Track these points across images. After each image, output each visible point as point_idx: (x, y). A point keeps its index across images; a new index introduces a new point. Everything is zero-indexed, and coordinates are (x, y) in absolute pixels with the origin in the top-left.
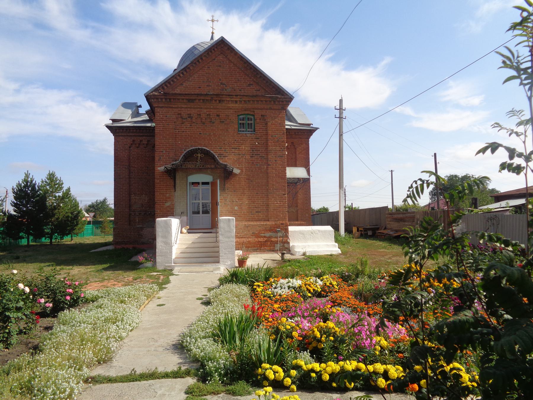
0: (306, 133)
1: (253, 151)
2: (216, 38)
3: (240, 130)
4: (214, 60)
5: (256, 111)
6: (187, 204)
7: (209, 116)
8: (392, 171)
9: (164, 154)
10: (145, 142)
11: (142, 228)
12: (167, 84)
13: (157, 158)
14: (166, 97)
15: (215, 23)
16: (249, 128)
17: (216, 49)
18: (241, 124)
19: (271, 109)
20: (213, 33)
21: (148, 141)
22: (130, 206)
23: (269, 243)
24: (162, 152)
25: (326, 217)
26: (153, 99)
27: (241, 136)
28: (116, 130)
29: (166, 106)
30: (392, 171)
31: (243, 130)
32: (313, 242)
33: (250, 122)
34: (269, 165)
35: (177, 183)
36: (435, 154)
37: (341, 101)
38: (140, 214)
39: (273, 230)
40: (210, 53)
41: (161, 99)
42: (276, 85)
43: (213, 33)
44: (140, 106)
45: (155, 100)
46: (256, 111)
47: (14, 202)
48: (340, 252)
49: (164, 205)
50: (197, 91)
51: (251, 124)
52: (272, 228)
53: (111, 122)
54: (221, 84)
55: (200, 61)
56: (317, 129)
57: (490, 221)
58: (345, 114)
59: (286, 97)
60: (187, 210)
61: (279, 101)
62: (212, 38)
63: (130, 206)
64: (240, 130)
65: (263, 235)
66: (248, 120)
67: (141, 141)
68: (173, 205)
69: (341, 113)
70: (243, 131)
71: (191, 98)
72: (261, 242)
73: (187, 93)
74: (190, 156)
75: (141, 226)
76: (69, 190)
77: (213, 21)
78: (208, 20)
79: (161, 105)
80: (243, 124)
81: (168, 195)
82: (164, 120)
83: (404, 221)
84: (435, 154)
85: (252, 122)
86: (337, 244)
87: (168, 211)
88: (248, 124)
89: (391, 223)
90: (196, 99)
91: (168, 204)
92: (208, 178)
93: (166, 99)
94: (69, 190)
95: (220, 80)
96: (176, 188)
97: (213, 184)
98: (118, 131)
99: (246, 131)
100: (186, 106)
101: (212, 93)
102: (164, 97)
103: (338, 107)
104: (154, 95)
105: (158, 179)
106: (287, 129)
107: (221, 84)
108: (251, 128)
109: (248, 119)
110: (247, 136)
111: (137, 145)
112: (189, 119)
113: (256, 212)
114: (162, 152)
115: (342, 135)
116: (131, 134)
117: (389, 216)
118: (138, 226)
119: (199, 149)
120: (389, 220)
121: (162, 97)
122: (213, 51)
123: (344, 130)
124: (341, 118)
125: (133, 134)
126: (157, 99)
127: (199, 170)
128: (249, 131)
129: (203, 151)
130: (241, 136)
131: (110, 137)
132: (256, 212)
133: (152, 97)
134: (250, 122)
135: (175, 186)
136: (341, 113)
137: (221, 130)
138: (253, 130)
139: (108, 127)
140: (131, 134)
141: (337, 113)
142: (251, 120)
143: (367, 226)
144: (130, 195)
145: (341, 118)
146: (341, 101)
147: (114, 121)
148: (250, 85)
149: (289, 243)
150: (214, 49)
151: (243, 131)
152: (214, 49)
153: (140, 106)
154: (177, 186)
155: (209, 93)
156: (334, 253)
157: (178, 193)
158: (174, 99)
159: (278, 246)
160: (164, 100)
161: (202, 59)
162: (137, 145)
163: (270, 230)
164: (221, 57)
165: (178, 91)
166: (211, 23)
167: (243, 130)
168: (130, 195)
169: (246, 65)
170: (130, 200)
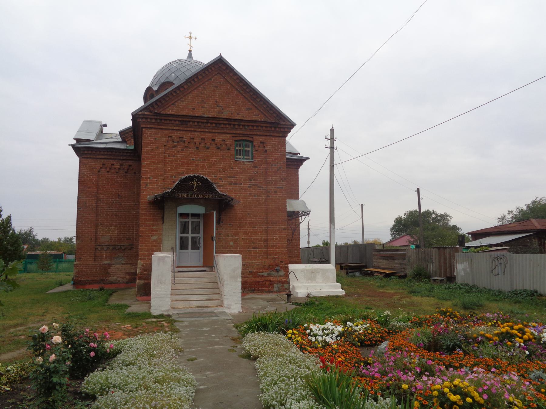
0: (296, 162)
1: (250, 180)
2: (205, 57)
3: (237, 157)
4: (210, 79)
6: (176, 238)
7: (203, 141)
8: (362, 205)
9: (152, 180)
10: (117, 166)
11: (110, 265)
12: (158, 103)
13: (143, 185)
14: (156, 117)
15: (193, 40)
16: (246, 156)
17: (213, 68)
18: (237, 150)
19: (271, 136)
20: (190, 51)
21: (121, 165)
22: (96, 239)
23: (267, 283)
24: (150, 178)
25: (319, 255)
26: (142, 118)
27: (238, 164)
28: (84, 151)
29: (156, 127)
30: (362, 205)
31: (240, 157)
32: (313, 281)
33: (247, 149)
34: (267, 196)
35: (165, 215)
36: (418, 189)
37: (332, 130)
38: (107, 248)
39: (272, 268)
40: (207, 73)
41: (151, 119)
42: (277, 111)
43: (190, 51)
44: (105, 126)
45: (144, 120)
47: (61, 240)
48: (344, 293)
50: (191, 113)
51: (249, 151)
52: (271, 267)
53: (75, 142)
54: (217, 106)
55: (196, 80)
56: (308, 158)
57: (496, 260)
58: (336, 144)
59: (288, 123)
60: (176, 245)
61: (280, 128)
62: (190, 56)
63: (96, 239)
64: (237, 157)
65: (261, 274)
66: (246, 147)
67: (113, 165)
68: (161, 239)
69: (332, 143)
70: (240, 158)
71: (185, 119)
72: (259, 282)
73: (179, 114)
74: (185, 184)
75: (108, 262)
76: (9, 218)
77: (190, 38)
78: (185, 37)
79: (149, 126)
80: (240, 150)
82: (154, 143)
83: (394, 259)
84: (418, 189)
85: (250, 149)
86: (340, 284)
87: (155, 246)
88: (246, 151)
89: (378, 261)
90: (189, 121)
91: (154, 238)
92: (200, 210)
93: (156, 119)
94: (9, 218)
95: (216, 102)
96: (165, 219)
97: (207, 217)
98: (86, 152)
99: (243, 159)
100: (178, 128)
101: (207, 116)
103: (329, 137)
105: (144, 209)
106: (287, 159)
107: (217, 106)
108: (248, 156)
109: (246, 146)
110: (244, 164)
111: (108, 170)
112: (181, 143)
113: (254, 248)
114: (150, 178)
115: (333, 166)
116: (101, 157)
117: (377, 253)
118: (105, 262)
119: (195, 176)
120: (376, 257)
121: (152, 117)
122: (210, 71)
123: (336, 161)
124: (332, 148)
125: (103, 157)
126: (147, 118)
127: (191, 201)
128: (246, 159)
129: (200, 179)
130: (238, 164)
131: (75, 160)
132: (254, 248)
133: (141, 116)
134: (247, 149)
135: (163, 218)
136: (332, 143)
137: (216, 156)
138: (250, 157)
139: (74, 146)
140: (101, 157)
141: (328, 143)
142: (249, 147)
143: (356, 262)
144: (97, 225)
145: (332, 148)
146: (332, 130)
147: (78, 140)
148: (248, 109)
149: (289, 283)
150: (211, 68)
151: (240, 158)
152: (211, 68)
153: (105, 126)
154: (165, 217)
155: (204, 116)
156: (339, 294)
157: (166, 226)
158: (165, 120)
159: (276, 287)
160: (153, 121)
161: (197, 77)
162: (108, 170)
163: (269, 269)
164: (218, 78)
165: (169, 111)
166: (188, 39)
167: (240, 157)
168: (97, 225)
169: (245, 87)
170: (96, 232)
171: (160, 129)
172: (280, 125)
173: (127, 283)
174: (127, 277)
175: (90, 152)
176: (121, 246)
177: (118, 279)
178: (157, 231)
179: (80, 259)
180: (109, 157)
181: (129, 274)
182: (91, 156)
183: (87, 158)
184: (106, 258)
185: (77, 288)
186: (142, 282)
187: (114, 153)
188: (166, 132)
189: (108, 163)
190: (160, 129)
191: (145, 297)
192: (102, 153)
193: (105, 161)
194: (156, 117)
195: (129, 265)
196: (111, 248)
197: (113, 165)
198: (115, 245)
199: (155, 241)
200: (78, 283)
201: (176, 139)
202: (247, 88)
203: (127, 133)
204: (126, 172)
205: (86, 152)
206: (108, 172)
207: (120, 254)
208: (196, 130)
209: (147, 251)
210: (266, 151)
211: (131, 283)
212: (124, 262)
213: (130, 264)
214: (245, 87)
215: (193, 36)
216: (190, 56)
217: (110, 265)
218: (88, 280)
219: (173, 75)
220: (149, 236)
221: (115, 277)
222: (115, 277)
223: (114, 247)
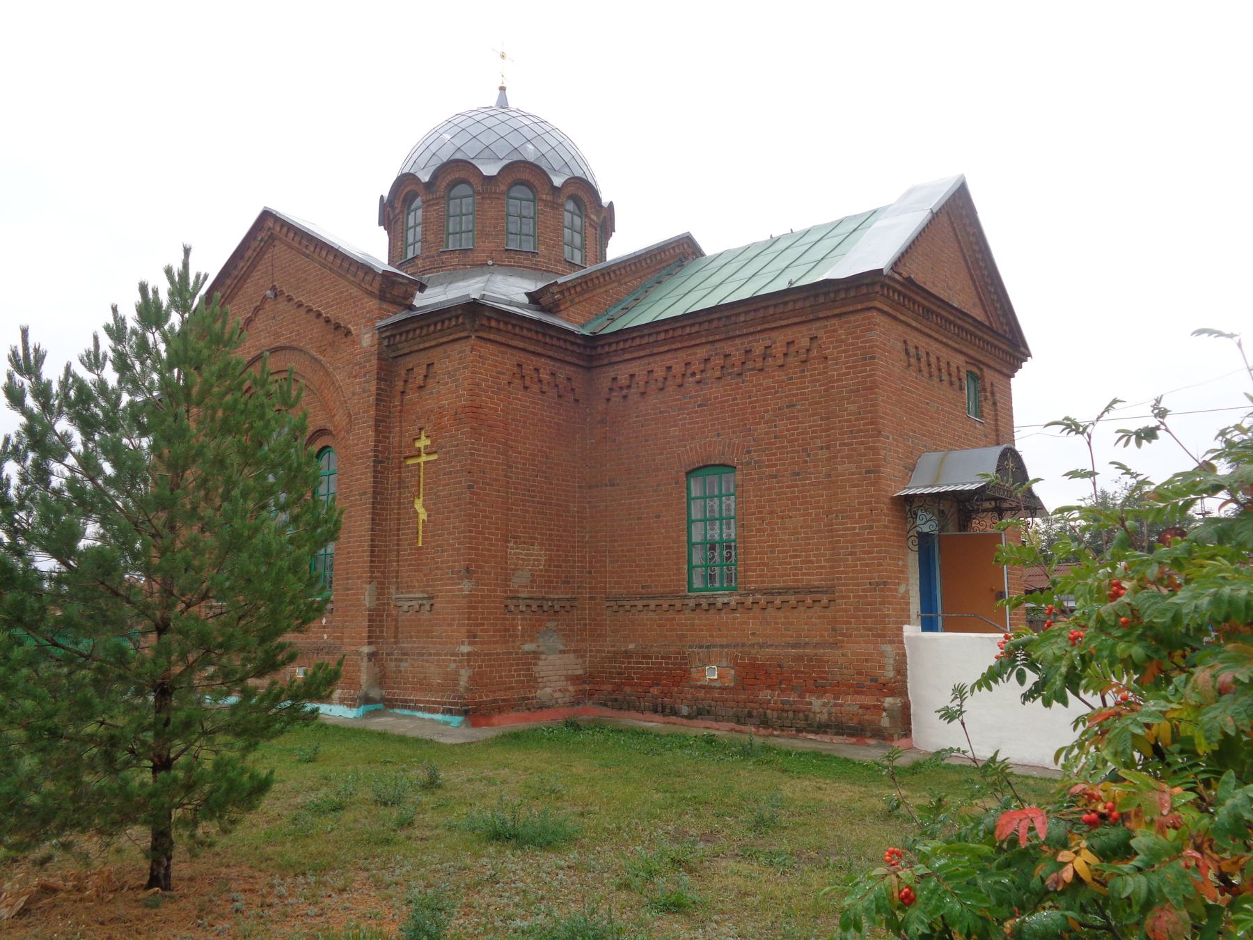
5: (985, 369)
10: (545, 376)
11: (536, 655)
20: (503, 89)
28: (489, 319)
43: (503, 89)
46: (985, 369)
49: (897, 590)
59: (1023, 349)
62: (503, 103)
81: (901, 563)
98: (493, 324)
102: (898, 287)
104: (890, 278)
121: (898, 287)
125: (521, 345)
126: (889, 288)
133: (887, 281)
171: (895, 318)
172: (1012, 349)
173: (572, 704)
174: (571, 688)
175: (502, 326)
176: (553, 600)
177: (557, 695)
178: (902, 572)
179: (475, 637)
180: (532, 348)
181: (575, 679)
182: (498, 338)
183: (490, 340)
184: (523, 636)
185: (475, 724)
186: (898, 701)
187: (548, 340)
188: (901, 328)
189: (530, 363)
190: (895, 318)
191: (904, 741)
192: (525, 332)
193: (522, 357)
194: (903, 290)
195: (572, 656)
196: (534, 608)
197: (537, 370)
198: (543, 598)
199: (902, 598)
200: (475, 711)
201: (912, 351)
202: (983, 259)
203: (568, 289)
204: (560, 396)
205: (493, 324)
206: (526, 388)
207: (551, 625)
208: (933, 334)
209: (896, 623)
210: (995, 404)
211: (578, 703)
212: (562, 648)
213: (575, 651)
214: (979, 256)
215: (508, 55)
216: (503, 103)
217: (536, 655)
218: (495, 701)
219: (530, 146)
220: (895, 584)
221: (548, 690)
222: (548, 690)
223: (539, 603)
